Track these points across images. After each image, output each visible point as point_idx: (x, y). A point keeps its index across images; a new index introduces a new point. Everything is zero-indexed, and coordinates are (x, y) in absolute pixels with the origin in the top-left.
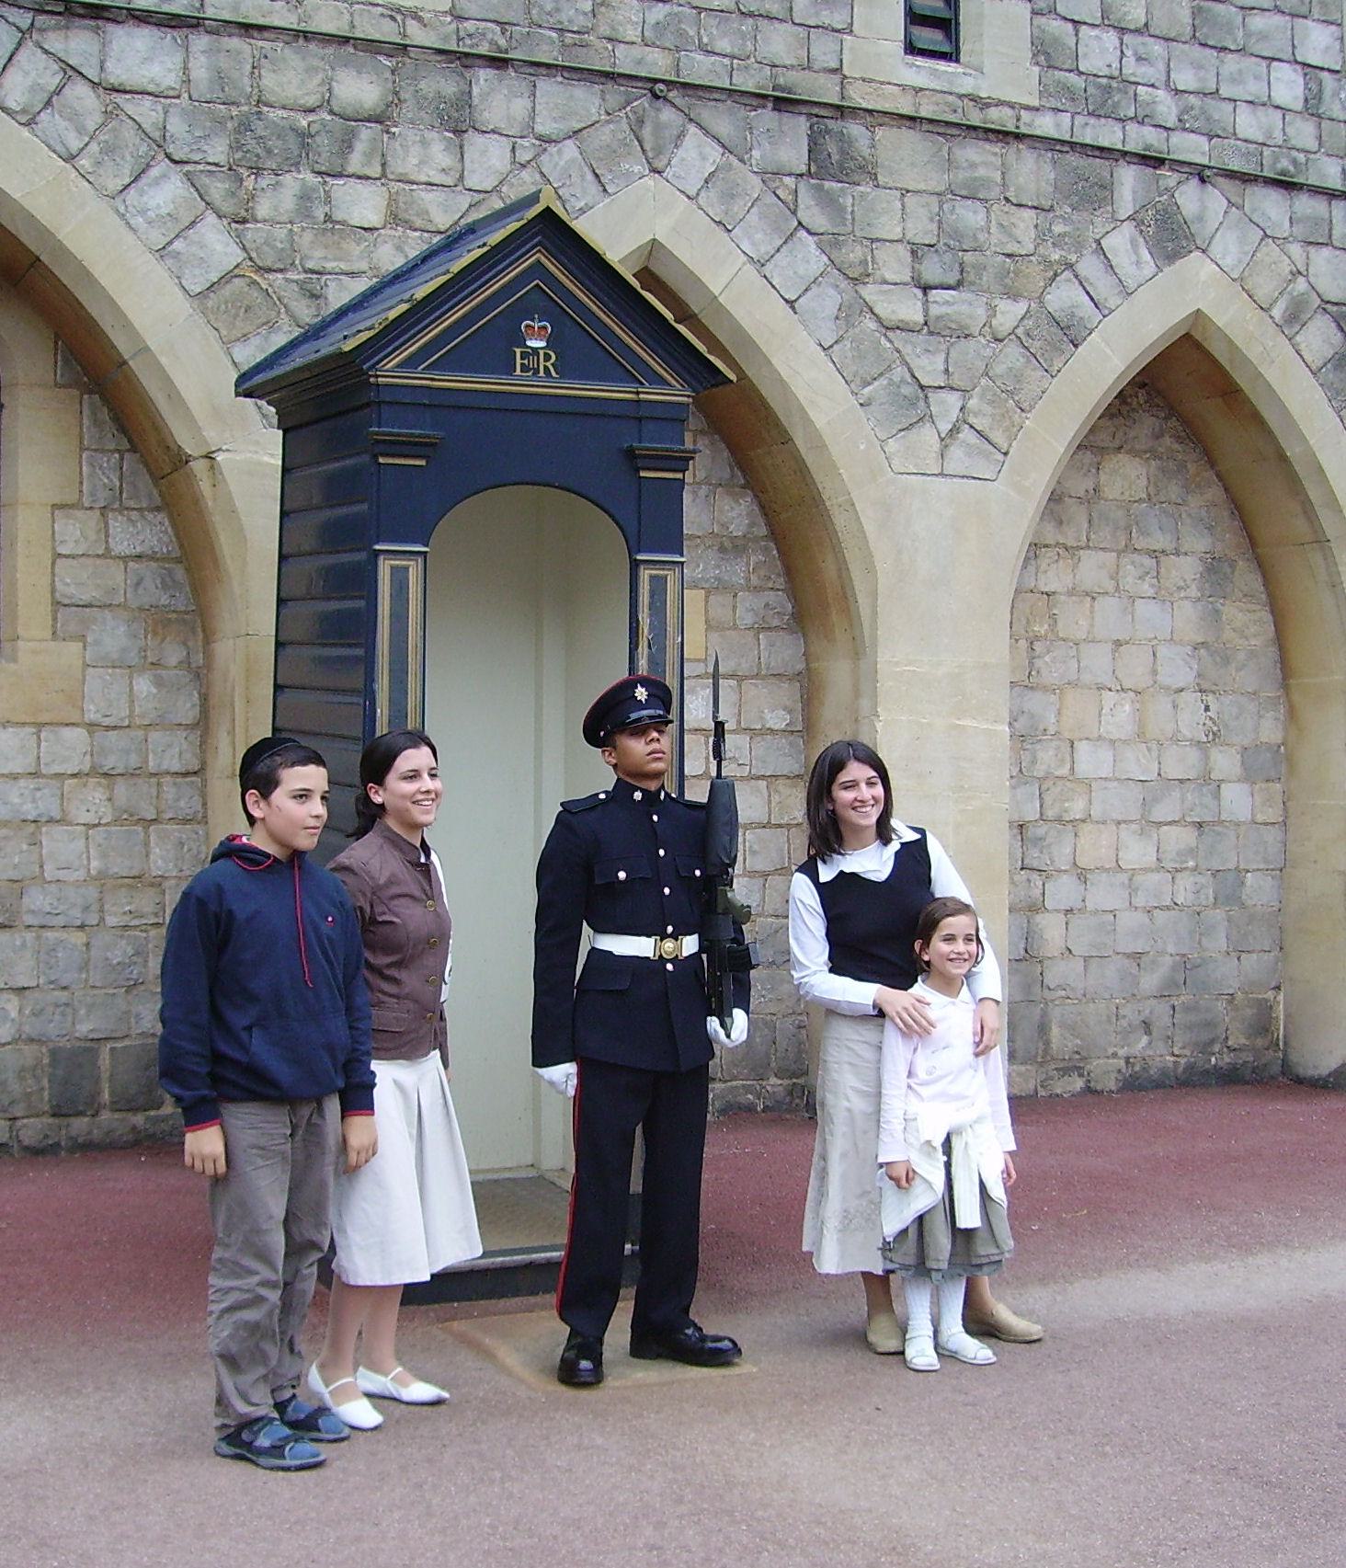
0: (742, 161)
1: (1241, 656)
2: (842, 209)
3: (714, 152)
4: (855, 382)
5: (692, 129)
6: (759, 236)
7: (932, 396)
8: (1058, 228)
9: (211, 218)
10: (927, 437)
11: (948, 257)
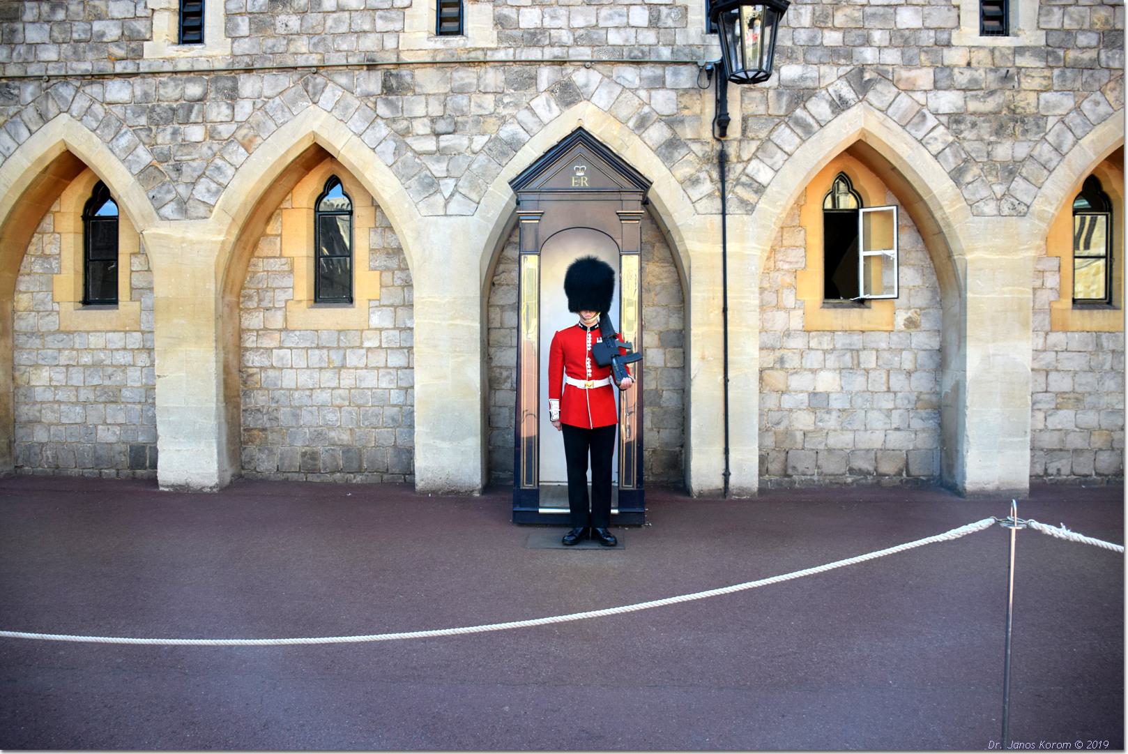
0: (353, 93)
1: (658, 288)
2: (397, 107)
3: (339, 93)
4: (404, 176)
5: (330, 84)
6: (359, 124)
7: (441, 182)
8: (506, 100)
9: (141, 146)
10: (439, 199)
11: (449, 120)
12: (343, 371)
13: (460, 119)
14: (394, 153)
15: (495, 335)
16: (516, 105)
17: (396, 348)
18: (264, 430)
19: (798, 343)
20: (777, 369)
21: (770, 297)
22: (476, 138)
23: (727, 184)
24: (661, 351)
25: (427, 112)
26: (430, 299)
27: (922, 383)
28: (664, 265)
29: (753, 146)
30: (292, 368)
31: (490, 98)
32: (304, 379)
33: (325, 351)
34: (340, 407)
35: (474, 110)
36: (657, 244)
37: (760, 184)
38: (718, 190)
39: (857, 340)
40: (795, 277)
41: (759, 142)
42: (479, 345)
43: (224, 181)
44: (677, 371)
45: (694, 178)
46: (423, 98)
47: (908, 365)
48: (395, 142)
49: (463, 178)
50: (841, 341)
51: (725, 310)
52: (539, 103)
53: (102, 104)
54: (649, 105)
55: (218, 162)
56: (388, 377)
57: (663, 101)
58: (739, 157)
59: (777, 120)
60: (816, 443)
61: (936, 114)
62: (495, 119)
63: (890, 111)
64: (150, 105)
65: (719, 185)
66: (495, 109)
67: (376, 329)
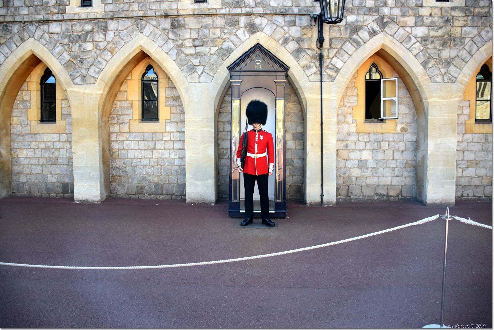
1: (292, 114)
2: (177, 34)
4: (181, 65)
6: (161, 42)
7: (197, 67)
8: (226, 31)
9: (65, 52)
10: (196, 75)
11: (200, 40)
12: (155, 151)
13: (205, 40)
14: (176, 55)
15: (221, 135)
16: (230, 33)
17: (178, 140)
18: (120, 176)
19: (354, 138)
20: (344, 150)
21: (341, 118)
22: (212, 48)
23: (323, 68)
24: (294, 141)
25: (191, 37)
26: (193, 119)
27: (408, 156)
28: (296, 104)
29: (335, 51)
30: (132, 149)
31: (219, 30)
32: (138, 154)
33: (146, 142)
34: (153, 166)
35: (211, 36)
36: (292, 95)
37: (337, 68)
38: (319, 71)
39: (380, 137)
40: (353, 109)
41: (337, 50)
42: (214, 139)
43: (102, 67)
44: (300, 150)
45: (308, 66)
46: (189, 30)
47: (402, 148)
48: (177, 50)
49: (206, 66)
50: (373, 137)
51: (322, 124)
52: (240, 33)
53: (48, 33)
54: (289, 33)
55: (99, 59)
56: (174, 153)
57: (295, 32)
58: (328, 56)
59: (345, 40)
60: (361, 182)
61: (416, 37)
62: (220, 40)
63: (395, 36)
64: (69, 34)
65: (319, 69)
66: (221, 35)
67: (169, 132)
